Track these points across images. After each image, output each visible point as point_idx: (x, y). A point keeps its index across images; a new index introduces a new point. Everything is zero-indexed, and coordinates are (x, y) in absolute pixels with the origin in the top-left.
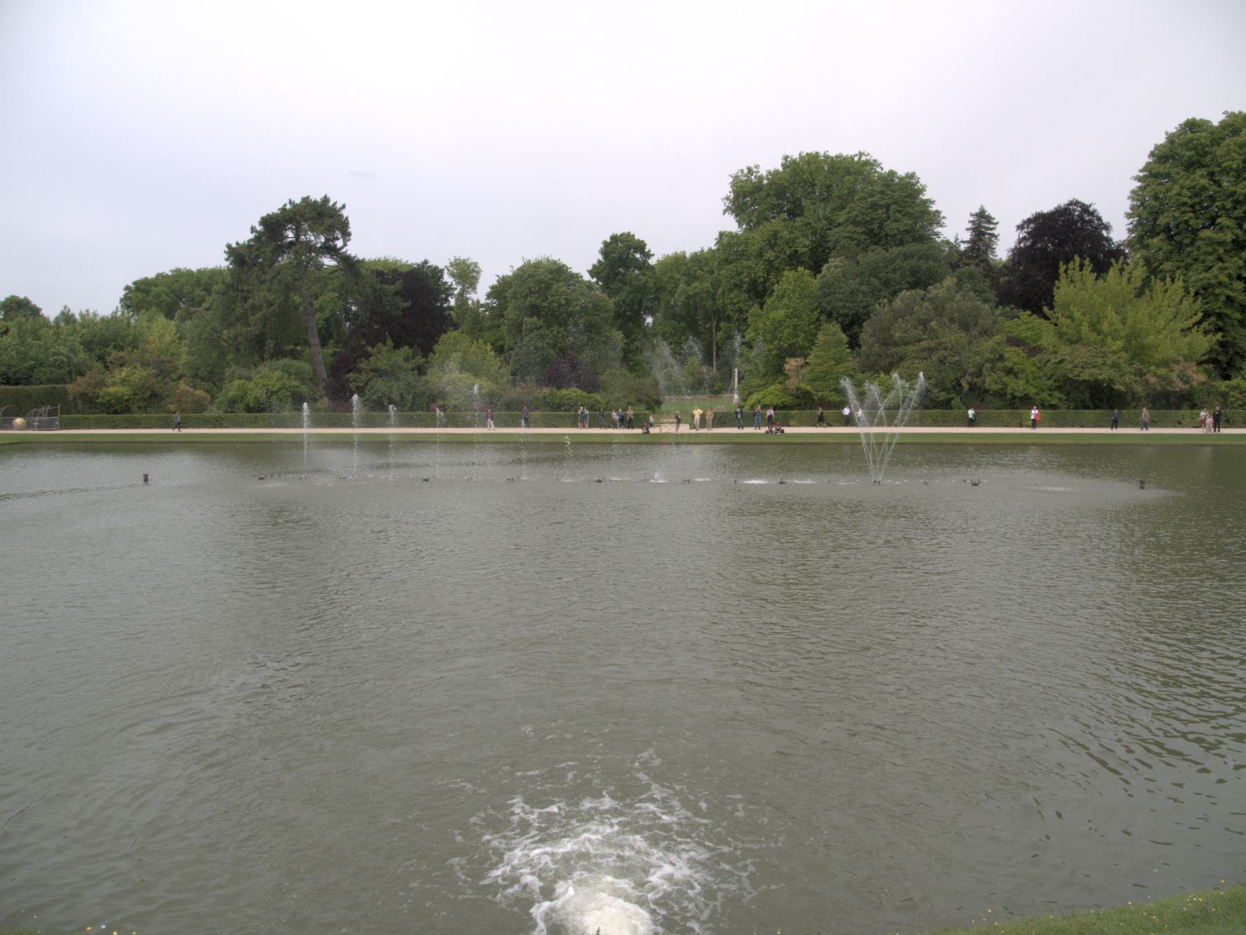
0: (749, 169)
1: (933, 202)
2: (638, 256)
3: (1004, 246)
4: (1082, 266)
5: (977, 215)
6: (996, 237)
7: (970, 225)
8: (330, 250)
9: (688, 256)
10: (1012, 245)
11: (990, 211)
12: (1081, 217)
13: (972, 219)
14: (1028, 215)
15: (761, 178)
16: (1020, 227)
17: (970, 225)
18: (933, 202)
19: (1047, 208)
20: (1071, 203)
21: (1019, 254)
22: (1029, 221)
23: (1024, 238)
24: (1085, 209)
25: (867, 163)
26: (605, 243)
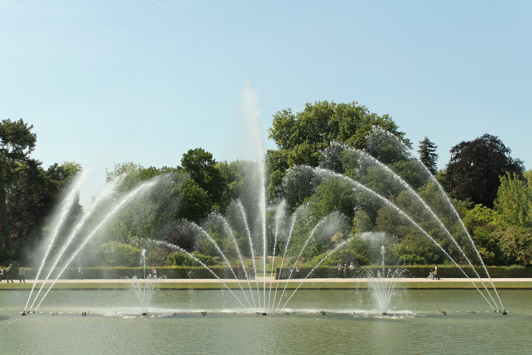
0: (285, 112)
1: (404, 134)
2: (207, 163)
3: (442, 162)
4: (512, 178)
5: (423, 142)
6: (436, 156)
7: (419, 149)
8: (18, 155)
9: (228, 164)
10: (448, 162)
11: (431, 140)
12: (491, 145)
13: (420, 145)
14: (458, 142)
15: (292, 117)
16: (452, 151)
17: (419, 149)
18: (404, 134)
19: (471, 138)
20: (485, 136)
21: (451, 167)
22: (457, 147)
23: (455, 158)
24: (494, 140)
25: (359, 109)
26: (185, 155)
